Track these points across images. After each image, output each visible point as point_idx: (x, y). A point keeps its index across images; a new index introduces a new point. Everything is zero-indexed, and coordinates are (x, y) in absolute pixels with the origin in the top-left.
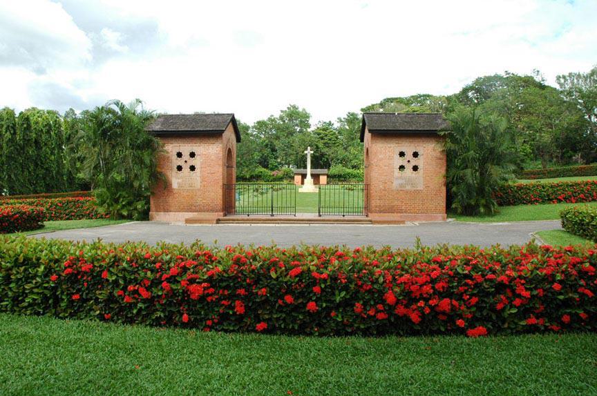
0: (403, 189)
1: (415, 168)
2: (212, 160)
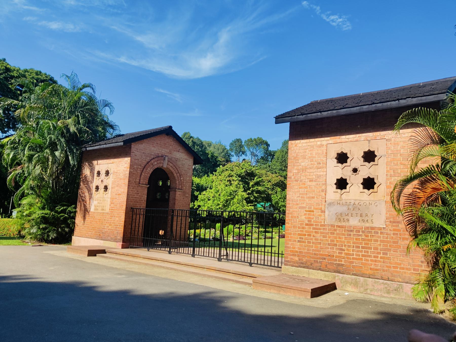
0: (343, 224)
1: (369, 184)
2: (121, 179)
